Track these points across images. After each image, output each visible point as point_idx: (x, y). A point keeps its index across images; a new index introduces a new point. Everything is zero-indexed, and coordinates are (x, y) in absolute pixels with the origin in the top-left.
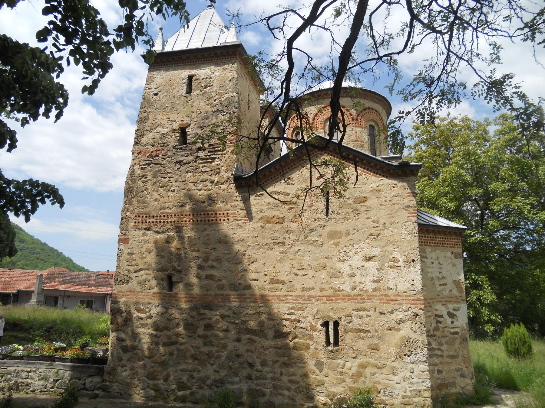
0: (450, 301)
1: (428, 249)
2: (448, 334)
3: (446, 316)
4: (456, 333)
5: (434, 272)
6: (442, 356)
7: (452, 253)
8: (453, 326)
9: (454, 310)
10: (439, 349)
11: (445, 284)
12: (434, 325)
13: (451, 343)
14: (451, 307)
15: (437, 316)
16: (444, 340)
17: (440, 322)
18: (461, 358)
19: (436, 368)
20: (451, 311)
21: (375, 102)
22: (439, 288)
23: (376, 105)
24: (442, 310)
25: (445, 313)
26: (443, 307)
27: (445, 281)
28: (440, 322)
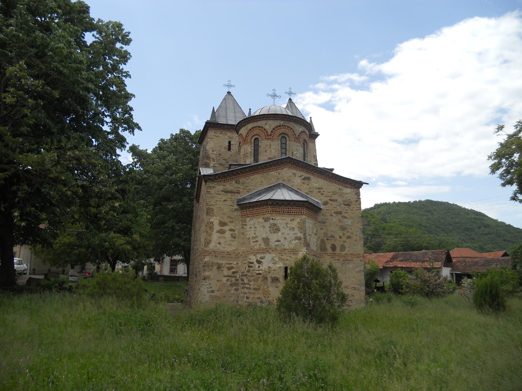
0: (259, 253)
1: (248, 219)
2: (255, 274)
3: (255, 263)
4: (260, 274)
5: (250, 234)
6: (250, 288)
7: (263, 218)
8: (259, 269)
9: (261, 258)
10: (248, 284)
11: (257, 241)
12: (247, 268)
13: (256, 280)
14: (259, 256)
15: (250, 263)
16: (252, 279)
17: (251, 267)
18: (261, 291)
19: (245, 295)
20: (259, 259)
21: (258, 121)
22: (253, 244)
23: (259, 122)
24: (253, 259)
25: (254, 261)
26: (254, 257)
27: (257, 239)
28: (251, 267)
